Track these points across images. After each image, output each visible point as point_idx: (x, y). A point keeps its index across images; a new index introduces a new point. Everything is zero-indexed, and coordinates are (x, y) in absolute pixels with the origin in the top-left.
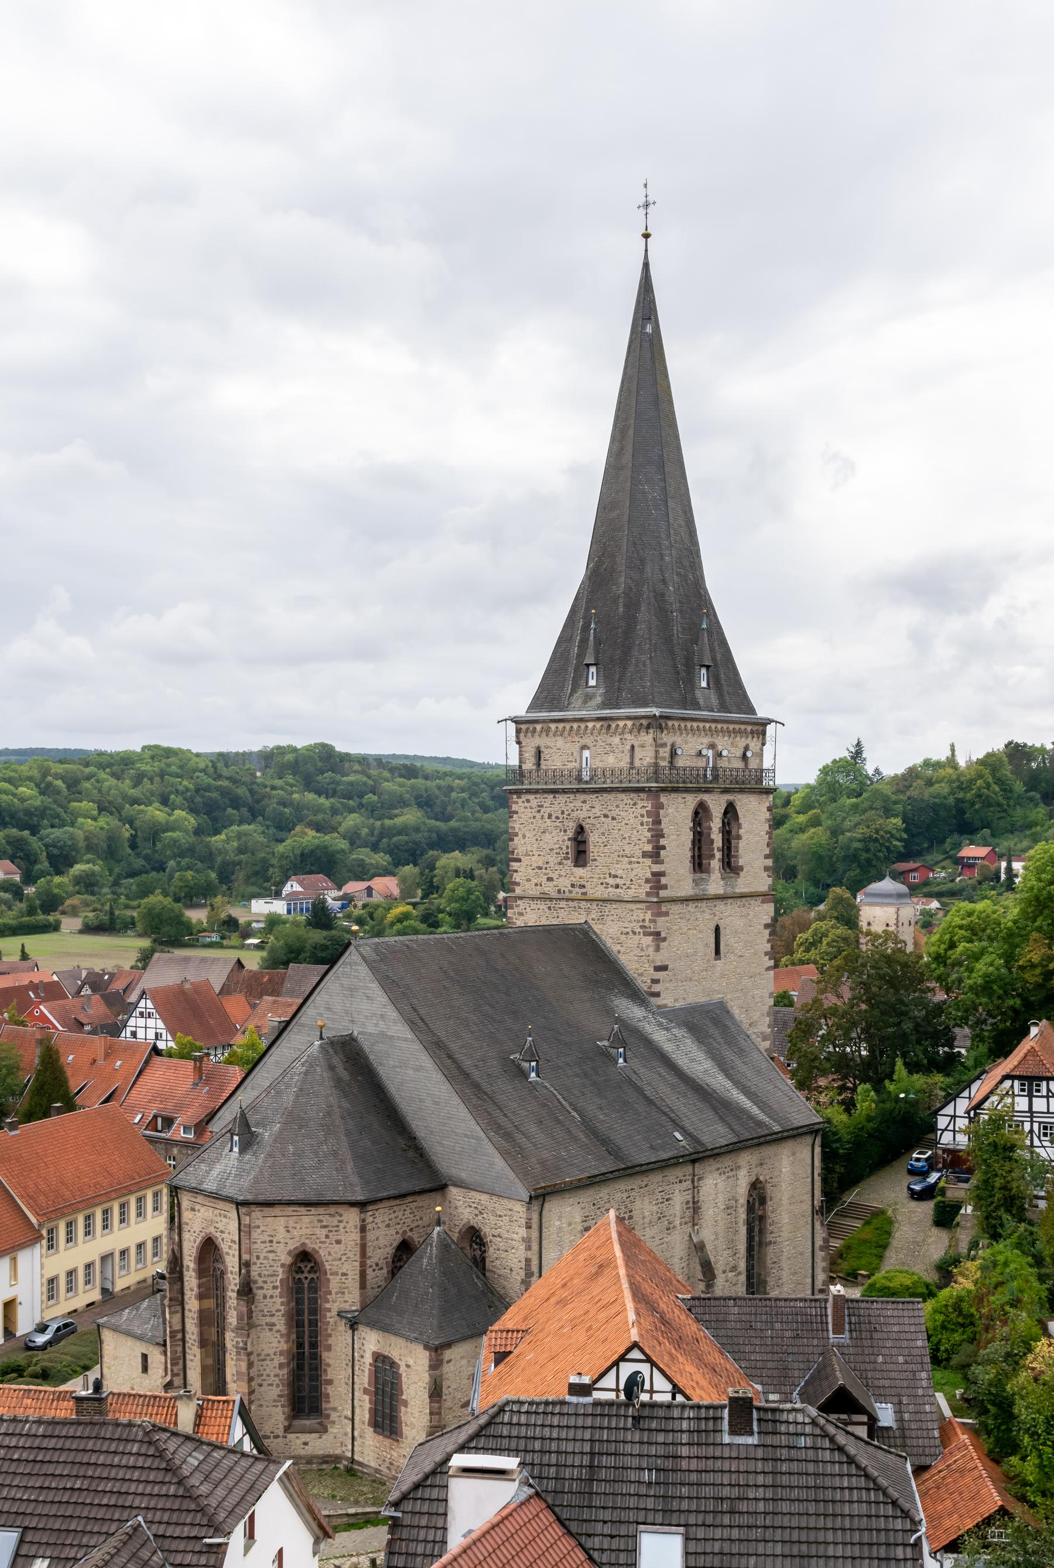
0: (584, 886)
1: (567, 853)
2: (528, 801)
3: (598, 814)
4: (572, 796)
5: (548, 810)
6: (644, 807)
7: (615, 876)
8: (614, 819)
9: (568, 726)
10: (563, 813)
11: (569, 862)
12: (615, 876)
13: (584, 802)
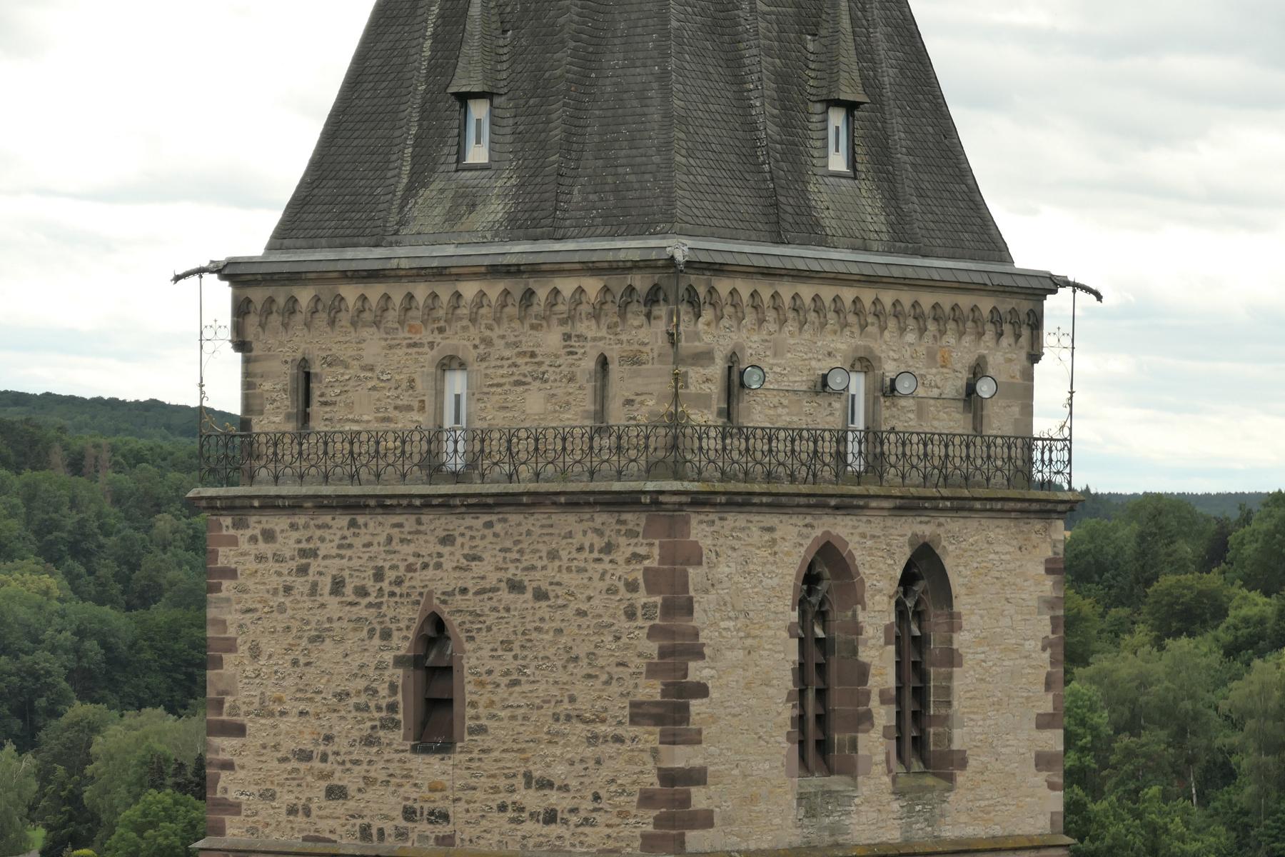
0: (445, 817)
1: (392, 708)
2: (269, 536)
3: (492, 579)
4: (409, 521)
5: (334, 566)
6: (636, 557)
7: (545, 784)
8: (540, 595)
9: (397, 293)
10: (379, 575)
11: (397, 736)
12: (545, 784)
13: (447, 540)
